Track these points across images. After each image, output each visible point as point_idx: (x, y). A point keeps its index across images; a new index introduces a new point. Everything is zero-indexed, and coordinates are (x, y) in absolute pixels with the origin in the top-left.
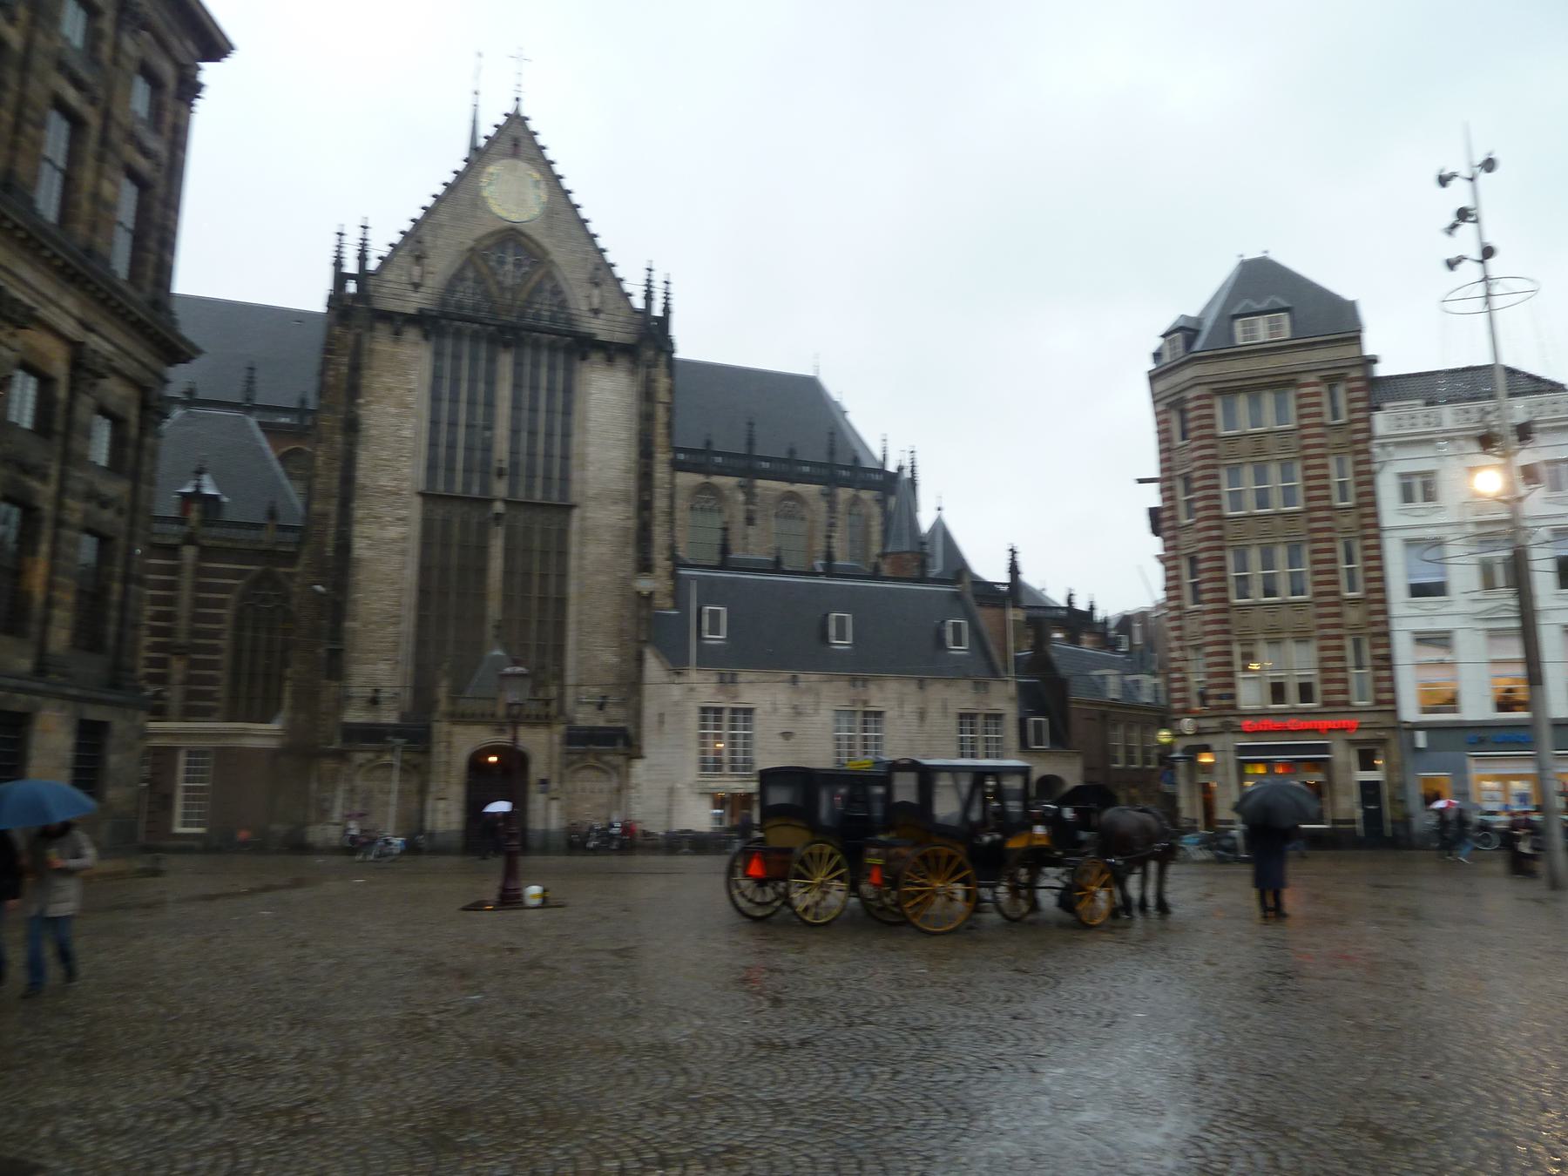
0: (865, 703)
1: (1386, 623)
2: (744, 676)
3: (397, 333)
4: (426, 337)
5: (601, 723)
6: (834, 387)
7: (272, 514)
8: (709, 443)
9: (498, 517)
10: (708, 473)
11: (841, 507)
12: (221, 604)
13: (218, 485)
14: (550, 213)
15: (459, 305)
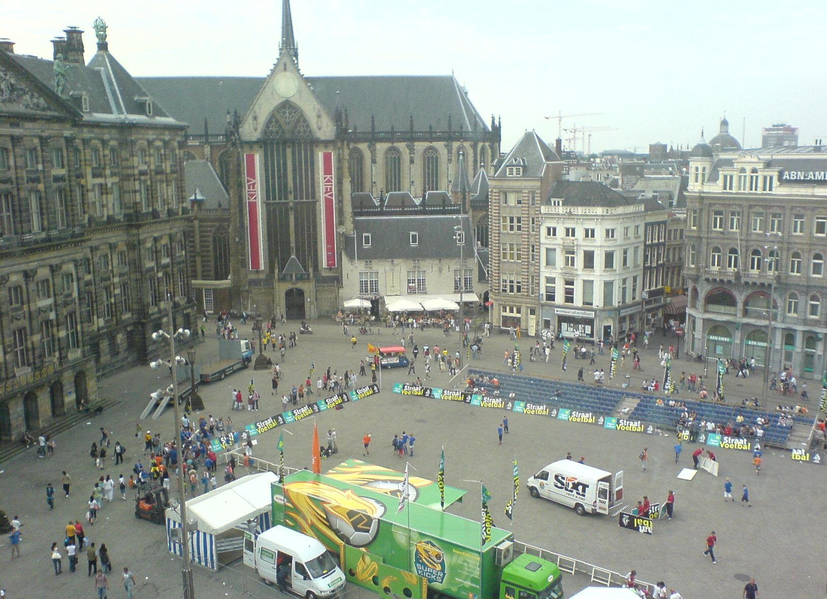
0: (419, 267)
1: (539, 272)
2: (374, 262)
3: (251, 148)
4: (261, 147)
5: (331, 275)
6: (461, 80)
7: (220, 205)
8: (392, 128)
9: (291, 208)
10: (393, 142)
11: (454, 151)
12: (209, 236)
13: (202, 194)
14: (299, 92)
15: (271, 132)
